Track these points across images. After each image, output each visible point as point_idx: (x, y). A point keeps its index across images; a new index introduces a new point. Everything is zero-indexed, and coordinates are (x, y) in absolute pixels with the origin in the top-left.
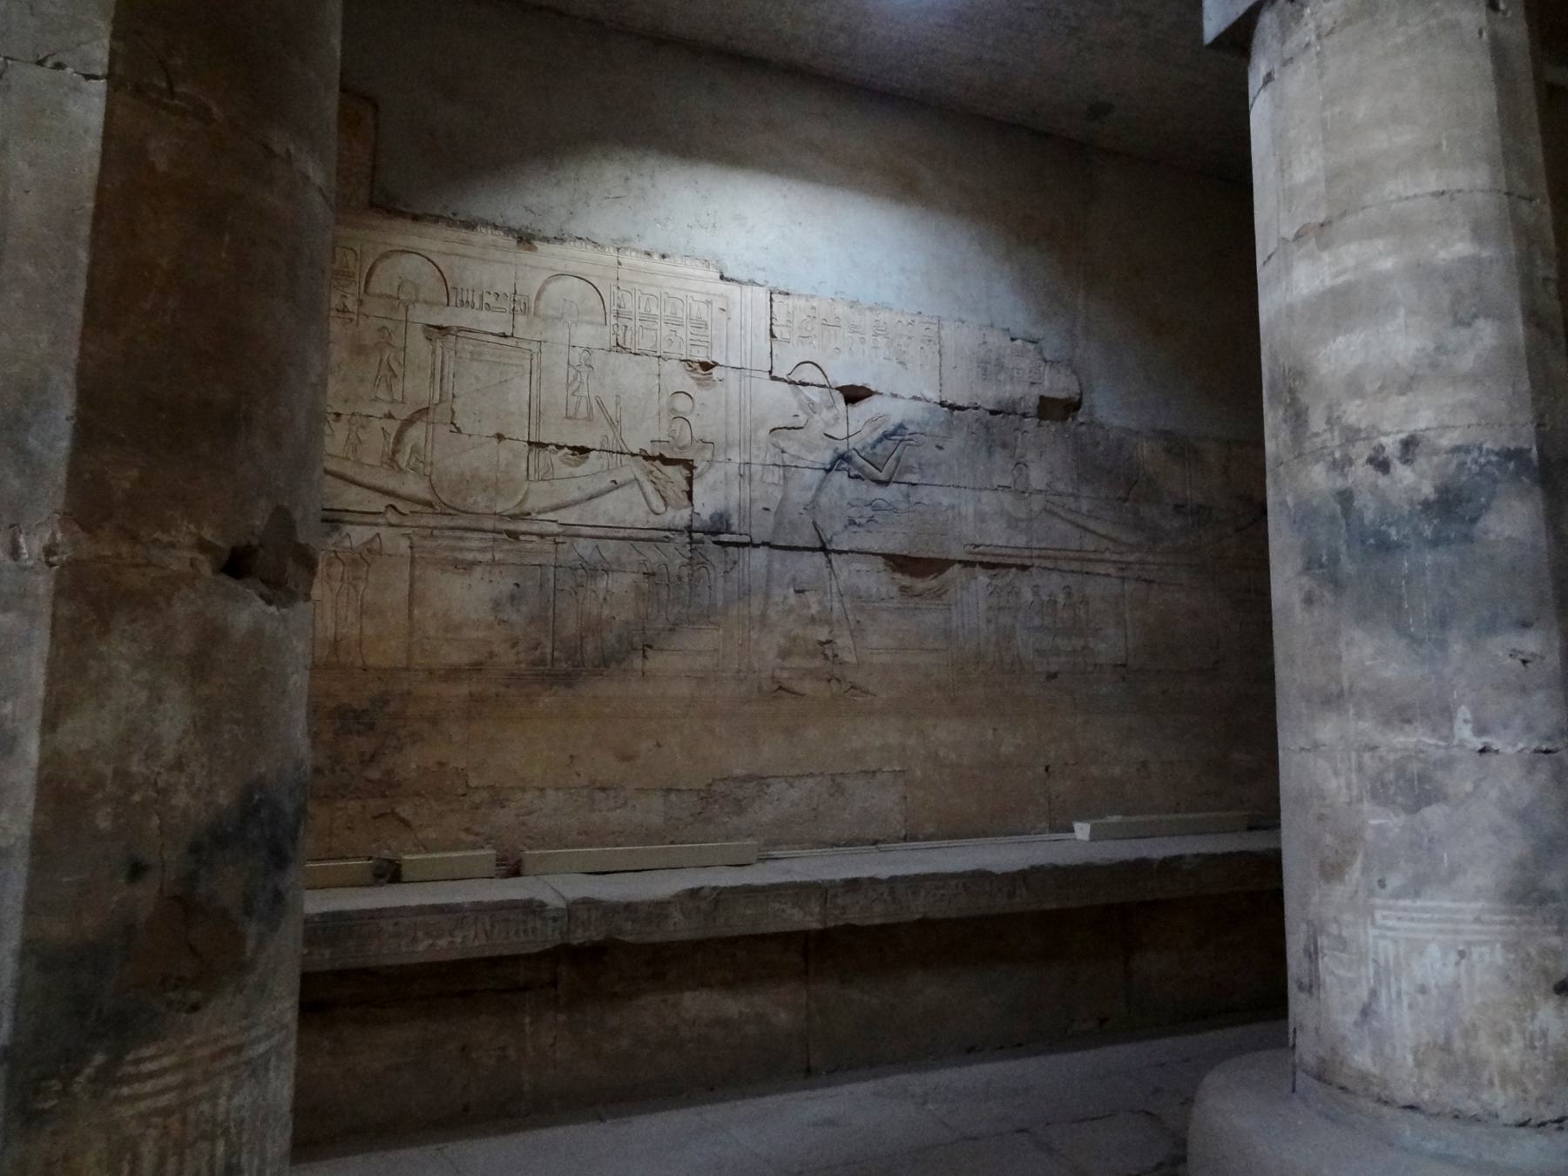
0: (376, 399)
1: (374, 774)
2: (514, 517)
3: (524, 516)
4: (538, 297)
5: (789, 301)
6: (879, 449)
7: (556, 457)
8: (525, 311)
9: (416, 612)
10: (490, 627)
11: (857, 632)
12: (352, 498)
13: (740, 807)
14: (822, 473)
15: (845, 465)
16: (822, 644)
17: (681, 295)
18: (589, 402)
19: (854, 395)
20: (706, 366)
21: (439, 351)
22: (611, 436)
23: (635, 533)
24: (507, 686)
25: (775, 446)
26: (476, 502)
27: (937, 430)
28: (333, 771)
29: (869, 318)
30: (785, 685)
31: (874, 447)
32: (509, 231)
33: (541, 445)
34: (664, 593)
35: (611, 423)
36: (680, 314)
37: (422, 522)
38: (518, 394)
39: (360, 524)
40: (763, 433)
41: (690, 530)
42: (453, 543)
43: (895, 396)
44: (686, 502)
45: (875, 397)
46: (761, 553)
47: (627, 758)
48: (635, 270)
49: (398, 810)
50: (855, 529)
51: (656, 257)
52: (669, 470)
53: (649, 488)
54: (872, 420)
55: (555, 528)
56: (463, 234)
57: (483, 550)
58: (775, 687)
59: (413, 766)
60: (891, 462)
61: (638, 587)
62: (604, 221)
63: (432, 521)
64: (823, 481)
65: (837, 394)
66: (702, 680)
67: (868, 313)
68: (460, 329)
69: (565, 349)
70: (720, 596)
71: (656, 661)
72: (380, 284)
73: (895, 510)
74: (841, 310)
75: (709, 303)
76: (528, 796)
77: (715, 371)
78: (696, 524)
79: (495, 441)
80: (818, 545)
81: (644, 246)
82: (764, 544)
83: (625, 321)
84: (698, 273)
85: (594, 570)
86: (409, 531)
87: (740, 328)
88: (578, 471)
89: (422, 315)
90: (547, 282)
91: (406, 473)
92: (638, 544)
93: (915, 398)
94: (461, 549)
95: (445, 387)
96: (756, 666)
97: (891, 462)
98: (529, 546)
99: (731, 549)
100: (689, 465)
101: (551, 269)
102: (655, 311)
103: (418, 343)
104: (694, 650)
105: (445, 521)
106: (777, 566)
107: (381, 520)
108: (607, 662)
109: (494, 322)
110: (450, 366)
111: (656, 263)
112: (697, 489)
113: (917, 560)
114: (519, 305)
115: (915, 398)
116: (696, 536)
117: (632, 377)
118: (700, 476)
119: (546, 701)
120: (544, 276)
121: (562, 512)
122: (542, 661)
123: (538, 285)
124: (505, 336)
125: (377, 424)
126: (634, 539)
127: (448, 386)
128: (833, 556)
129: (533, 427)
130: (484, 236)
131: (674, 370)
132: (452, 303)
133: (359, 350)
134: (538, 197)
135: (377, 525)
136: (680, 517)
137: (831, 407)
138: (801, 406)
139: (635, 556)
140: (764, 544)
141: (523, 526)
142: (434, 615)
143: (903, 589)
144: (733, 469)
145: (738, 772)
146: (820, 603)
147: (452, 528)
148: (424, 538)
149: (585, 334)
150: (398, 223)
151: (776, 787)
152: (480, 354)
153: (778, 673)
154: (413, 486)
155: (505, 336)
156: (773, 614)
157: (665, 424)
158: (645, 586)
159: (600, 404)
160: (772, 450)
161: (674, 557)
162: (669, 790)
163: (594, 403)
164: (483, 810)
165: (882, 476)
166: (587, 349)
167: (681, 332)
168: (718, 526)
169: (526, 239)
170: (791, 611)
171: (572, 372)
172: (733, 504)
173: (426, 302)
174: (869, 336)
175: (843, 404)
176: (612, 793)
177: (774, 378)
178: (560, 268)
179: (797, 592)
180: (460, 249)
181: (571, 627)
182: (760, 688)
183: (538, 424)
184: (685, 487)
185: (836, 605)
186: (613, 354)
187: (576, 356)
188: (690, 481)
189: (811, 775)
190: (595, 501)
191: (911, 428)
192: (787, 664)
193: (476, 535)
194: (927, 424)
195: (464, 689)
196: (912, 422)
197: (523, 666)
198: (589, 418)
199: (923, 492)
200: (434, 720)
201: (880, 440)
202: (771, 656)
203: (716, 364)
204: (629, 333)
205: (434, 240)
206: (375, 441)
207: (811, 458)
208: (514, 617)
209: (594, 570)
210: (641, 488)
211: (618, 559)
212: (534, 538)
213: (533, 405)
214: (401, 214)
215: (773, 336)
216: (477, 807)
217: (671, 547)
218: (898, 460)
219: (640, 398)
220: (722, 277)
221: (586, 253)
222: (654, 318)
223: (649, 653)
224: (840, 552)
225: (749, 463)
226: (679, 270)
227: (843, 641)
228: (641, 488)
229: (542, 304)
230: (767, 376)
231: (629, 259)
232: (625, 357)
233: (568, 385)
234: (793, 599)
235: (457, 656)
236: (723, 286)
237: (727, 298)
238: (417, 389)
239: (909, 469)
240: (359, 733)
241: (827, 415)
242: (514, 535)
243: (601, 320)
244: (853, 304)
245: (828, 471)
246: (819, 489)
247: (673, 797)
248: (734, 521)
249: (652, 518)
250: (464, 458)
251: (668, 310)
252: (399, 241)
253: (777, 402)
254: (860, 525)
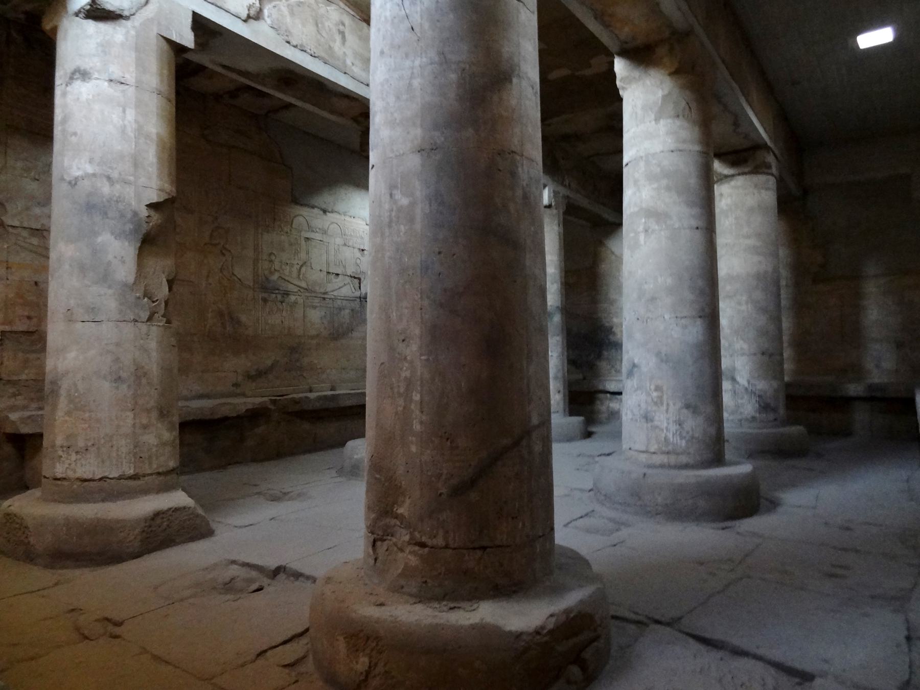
1: (298, 364)
3: (325, 293)
12: (291, 288)
100: (360, 279)
130: (316, 211)
131: (356, 251)
133: (291, 245)
134: (325, 199)
136: (357, 294)
141: (326, 296)
149: (339, 241)
154: (304, 285)
205: (305, 211)
221: (337, 216)
242: (324, 299)
250: (314, 275)
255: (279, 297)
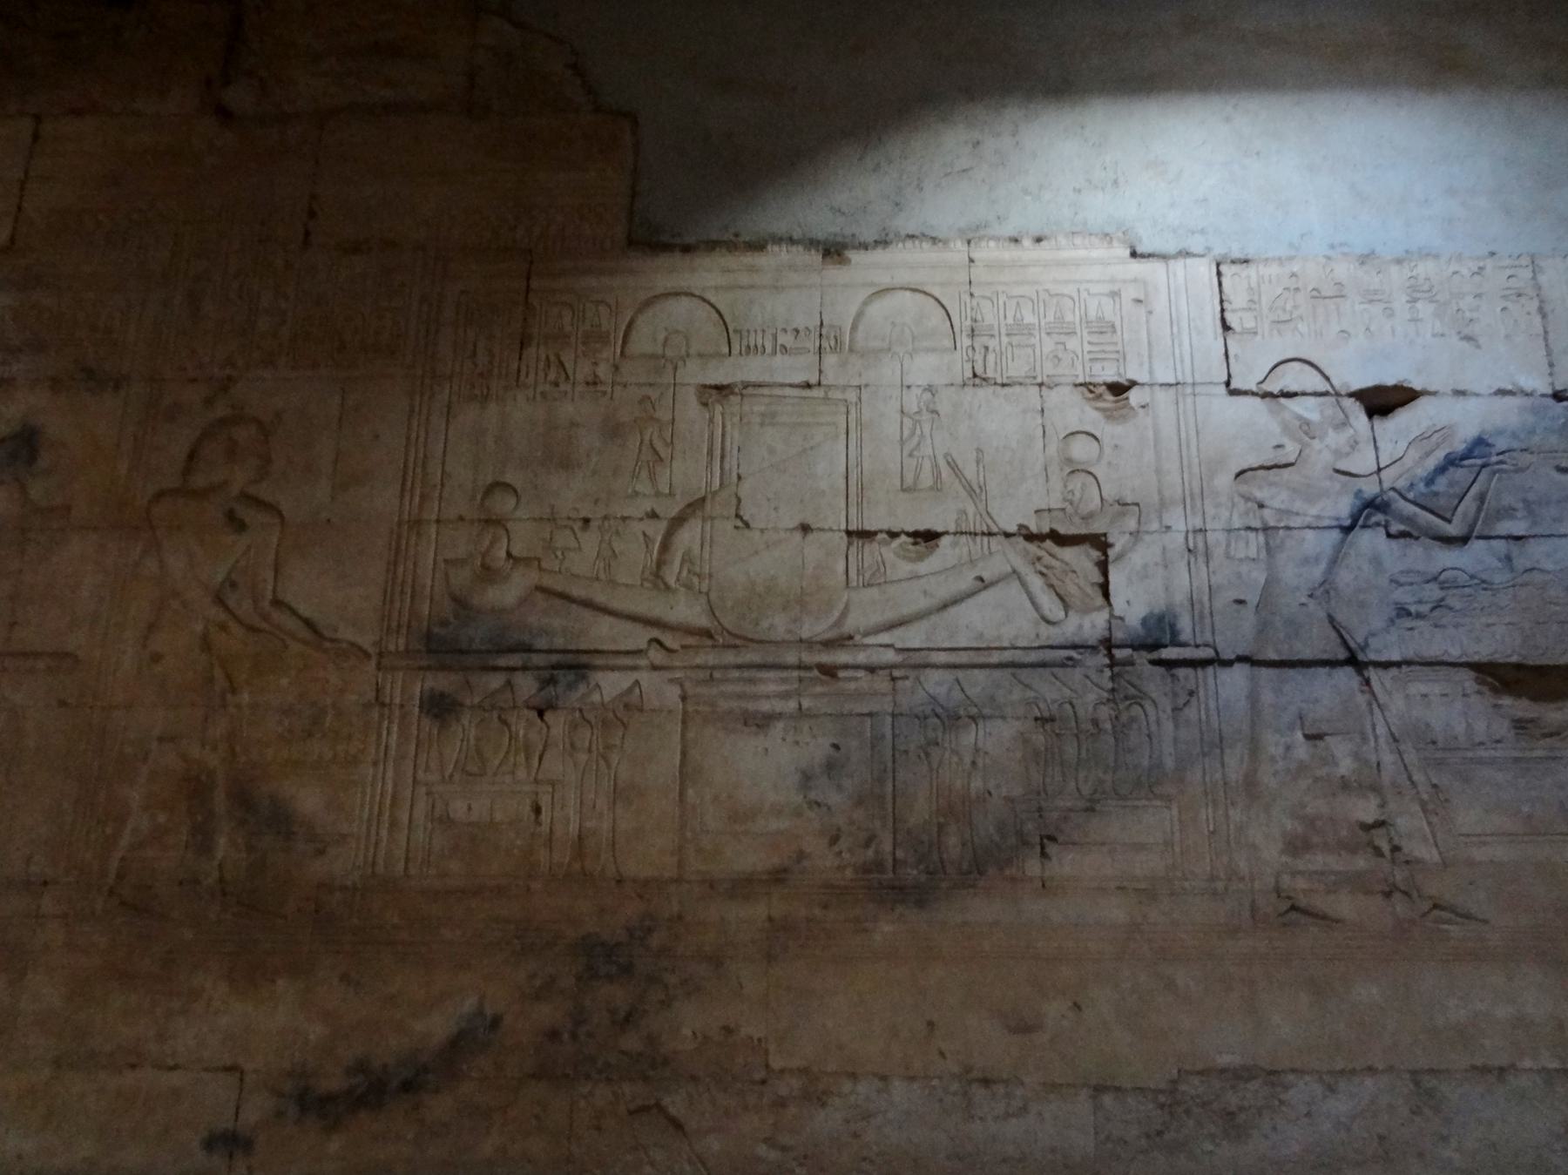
0: (636, 494)
1: (631, 1042)
2: (828, 644)
4: (854, 328)
5: (1251, 271)
6: (1441, 484)
7: (889, 552)
8: (837, 347)
9: (690, 792)
10: (798, 813)
11: (1435, 804)
12: (604, 633)
13: (1233, 1124)
14: (1336, 535)
15: (1379, 517)
16: (1367, 827)
17: (1070, 289)
18: (936, 466)
19: (1382, 402)
20: (1119, 389)
21: (718, 419)
22: (971, 510)
23: (1018, 656)
24: (825, 907)
25: (1247, 499)
26: (771, 626)
27: (1553, 440)
28: (574, 1036)
29: (1397, 276)
30: (1303, 902)
31: (1430, 481)
32: (812, 243)
33: (866, 535)
34: (1070, 750)
35: (971, 492)
36: (1069, 318)
37: (699, 660)
38: (829, 465)
39: (612, 669)
40: (1224, 481)
41: (1108, 644)
42: (738, 688)
43: (1460, 393)
44: (1100, 600)
45: (1422, 401)
46: (1239, 673)
47: (1024, 1028)
48: (998, 266)
49: (666, 1101)
50: (1408, 623)
51: (1027, 243)
52: (1068, 553)
53: (1036, 583)
54: (1423, 438)
55: (890, 656)
56: (749, 259)
57: (785, 696)
58: (1285, 906)
59: (687, 1032)
60: (1469, 504)
61: (1026, 741)
62: (943, 207)
63: (711, 658)
64: (1343, 541)
65: (1350, 403)
66: (1148, 893)
67: (1394, 269)
68: (746, 385)
69: (897, 392)
70: (1168, 748)
71: (1065, 863)
72: (642, 342)
73: (1485, 585)
74: (1343, 270)
75: (1115, 295)
76: (862, 1088)
77: (1134, 396)
78: (1119, 635)
79: (798, 536)
80: (1342, 654)
81: (1009, 230)
82: (1242, 659)
83: (985, 340)
84: (1095, 254)
85: (952, 719)
86: (678, 675)
87: (1171, 324)
88: (922, 567)
89: (695, 374)
90: (866, 303)
91: (674, 591)
92: (1024, 674)
93: (1502, 392)
94: (756, 697)
95: (727, 467)
96: (1243, 867)
97: (1469, 504)
98: (852, 686)
99: (1181, 672)
100: (1100, 543)
101: (872, 284)
102: (1029, 318)
103: (690, 409)
104: (1141, 837)
105: (730, 657)
106: (1267, 697)
107: (643, 662)
108: (984, 866)
109: (793, 369)
110: (735, 435)
111: (1028, 251)
112: (1116, 577)
113: (1541, 671)
114: (826, 340)
115: (1502, 392)
116: (1119, 654)
117: (1000, 420)
118: (1120, 557)
119: (886, 929)
120: (863, 294)
121: (898, 632)
122: (878, 865)
123: (853, 310)
124: (808, 386)
125: (637, 527)
126: (1015, 665)
127: (731, 462)
128: (1372, 673)
129: (853, 510)
130: (779, 255)
132: (735, 351)
133: (614, 431)
134: (847, 194)
135: (635, 668)
136: (1093, 625)
137: (1345, 423)
138: (1286, 429)
139: (1017, 695)
140: (1242, 659)
141: (842, 657)
142: (716, 798)
143: (1520, 725)
144: (1176, 540)
145: (1225, 1060)
146: (1356, 756)
147: (739, 667)
148: (699, 683)
149: (925, 368)
150: (663, 260)
151: (1301, 1091)
152: (774, 415)
153: (1286, 880)
154: (686, 611)
155: (808, 386)
156: (1267, 778)
157: (1056, 483)
158: (1039, 739)
159: (953, 466)
160: (1242, 505)
161: (1086, 690)
162: (1099, 1089)
163: (942, 463)
164: (793, 1110)
165: (1453, 529)
166: (930, 389)
167: (1073, 343)
168: (1156, 637)
169: (834, 251)
170: (1302, 768)
171: (908, 422)
172: (1180, 597)
173: (700, 355)
174: (1400, 302)
175: (1364, 418)
176: (1000, 1089)
177: (1235, 393)
178: (885, 280)
179: (1308, 737)
180: (744, 279)
181: (920, 811)
182: (1254, 909)
183: (859, 505)
184: (1097, 577)
185: (1388, 758)
186: (969, 390)
187: (912, 401)
188: (1103, 567)
189: (1371, 1070)
190: (953, 610)
191: (1501, 444)
192: (1300, 864)
193: (772, 674)
194: (1532, 432)
195: (758, 911)
196: (1500, 432)
197: (849, 873)
198: (937, 488)
199: (1537, 552)
200: (716, 961)
201: (1441, 470)
202: (1272, 853)
203: (1133, 384)
204: (991, 358)
205: (708, 274)
206: (634, 554)
207: (1314, 511)
208: (834, 798)
209: (952, 719)
210: (1024, 584)
211: (992, 698)
212: (861, 674)
213: (852, 482)
214: (667, 248)
215: (1226, 327)
216: (781, 1103)
217: (1077, 674)
218: (1482, 498)
219: (1016, 451)
220: (1134, 254)
221: (923, 254)
222: (1028, 330)
223: (1052, 849)
224: (1386, 665)
225: (1203, 531)
226: (1065, 254)
227: (1409, 822)
228: (1024, 584)
229: (860, 335)
230: (1223, 389)
231: (987, 252)
232: (984, 393)
233: (902, 441)
234: (1302, 751)
235: (749, 859)
236: (1137, 267)
237: (1145, 283)
238: (687, 473)
239: (1508, 513)
240: (610, 978)
241: (1335, 439)
242: (829, 671)
243: (948, 343)
244: (1364, 259)
245: (1347, 530)
246: (1334, 562)
247: (1107, 1100)
248: (1185, 625)
249: (1045, 631)
250: (748, 564)
251: (1050, 318)
252: (663, 283)
253: (1246, 428)
254: (1419, 616)
255: (526, 685)
